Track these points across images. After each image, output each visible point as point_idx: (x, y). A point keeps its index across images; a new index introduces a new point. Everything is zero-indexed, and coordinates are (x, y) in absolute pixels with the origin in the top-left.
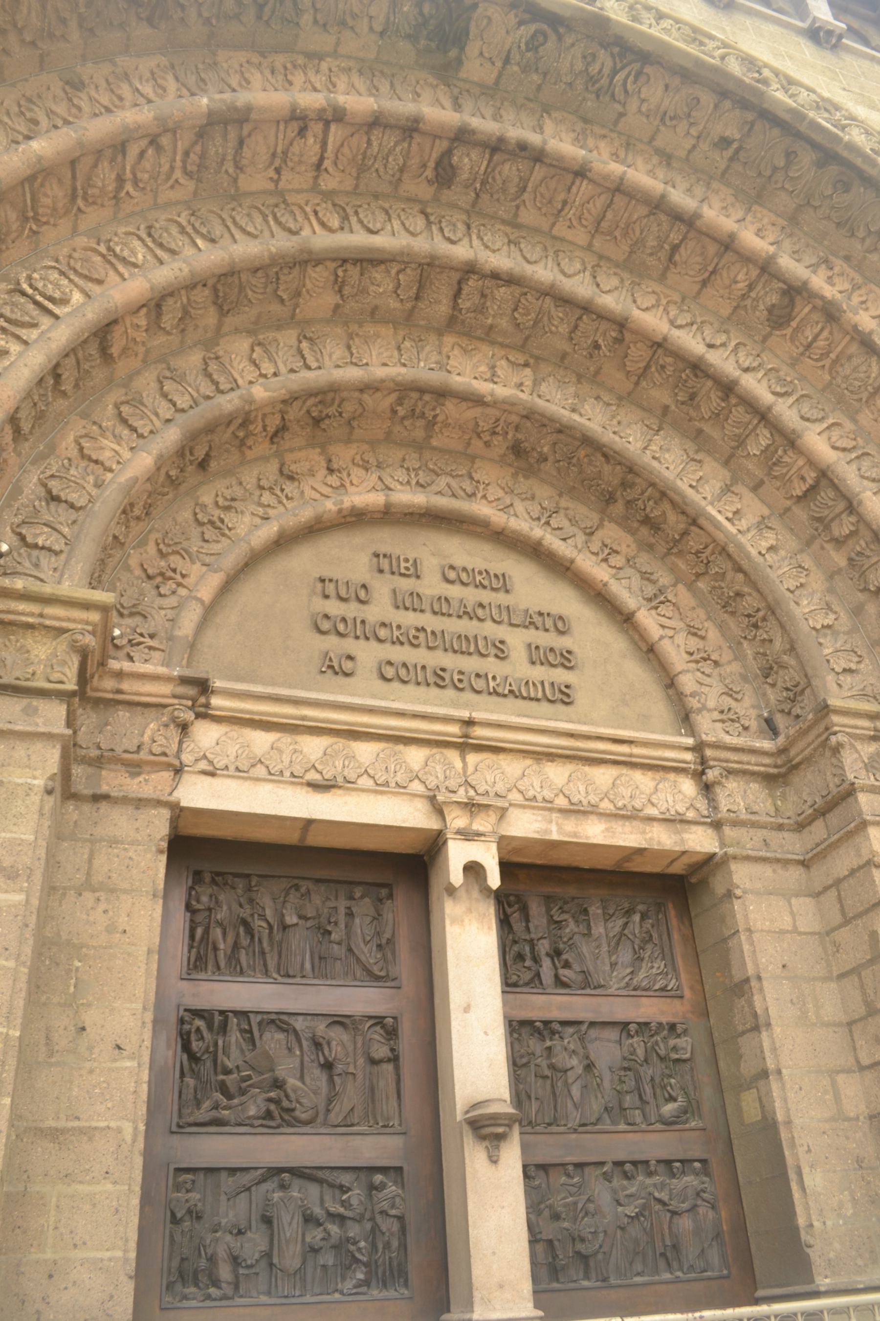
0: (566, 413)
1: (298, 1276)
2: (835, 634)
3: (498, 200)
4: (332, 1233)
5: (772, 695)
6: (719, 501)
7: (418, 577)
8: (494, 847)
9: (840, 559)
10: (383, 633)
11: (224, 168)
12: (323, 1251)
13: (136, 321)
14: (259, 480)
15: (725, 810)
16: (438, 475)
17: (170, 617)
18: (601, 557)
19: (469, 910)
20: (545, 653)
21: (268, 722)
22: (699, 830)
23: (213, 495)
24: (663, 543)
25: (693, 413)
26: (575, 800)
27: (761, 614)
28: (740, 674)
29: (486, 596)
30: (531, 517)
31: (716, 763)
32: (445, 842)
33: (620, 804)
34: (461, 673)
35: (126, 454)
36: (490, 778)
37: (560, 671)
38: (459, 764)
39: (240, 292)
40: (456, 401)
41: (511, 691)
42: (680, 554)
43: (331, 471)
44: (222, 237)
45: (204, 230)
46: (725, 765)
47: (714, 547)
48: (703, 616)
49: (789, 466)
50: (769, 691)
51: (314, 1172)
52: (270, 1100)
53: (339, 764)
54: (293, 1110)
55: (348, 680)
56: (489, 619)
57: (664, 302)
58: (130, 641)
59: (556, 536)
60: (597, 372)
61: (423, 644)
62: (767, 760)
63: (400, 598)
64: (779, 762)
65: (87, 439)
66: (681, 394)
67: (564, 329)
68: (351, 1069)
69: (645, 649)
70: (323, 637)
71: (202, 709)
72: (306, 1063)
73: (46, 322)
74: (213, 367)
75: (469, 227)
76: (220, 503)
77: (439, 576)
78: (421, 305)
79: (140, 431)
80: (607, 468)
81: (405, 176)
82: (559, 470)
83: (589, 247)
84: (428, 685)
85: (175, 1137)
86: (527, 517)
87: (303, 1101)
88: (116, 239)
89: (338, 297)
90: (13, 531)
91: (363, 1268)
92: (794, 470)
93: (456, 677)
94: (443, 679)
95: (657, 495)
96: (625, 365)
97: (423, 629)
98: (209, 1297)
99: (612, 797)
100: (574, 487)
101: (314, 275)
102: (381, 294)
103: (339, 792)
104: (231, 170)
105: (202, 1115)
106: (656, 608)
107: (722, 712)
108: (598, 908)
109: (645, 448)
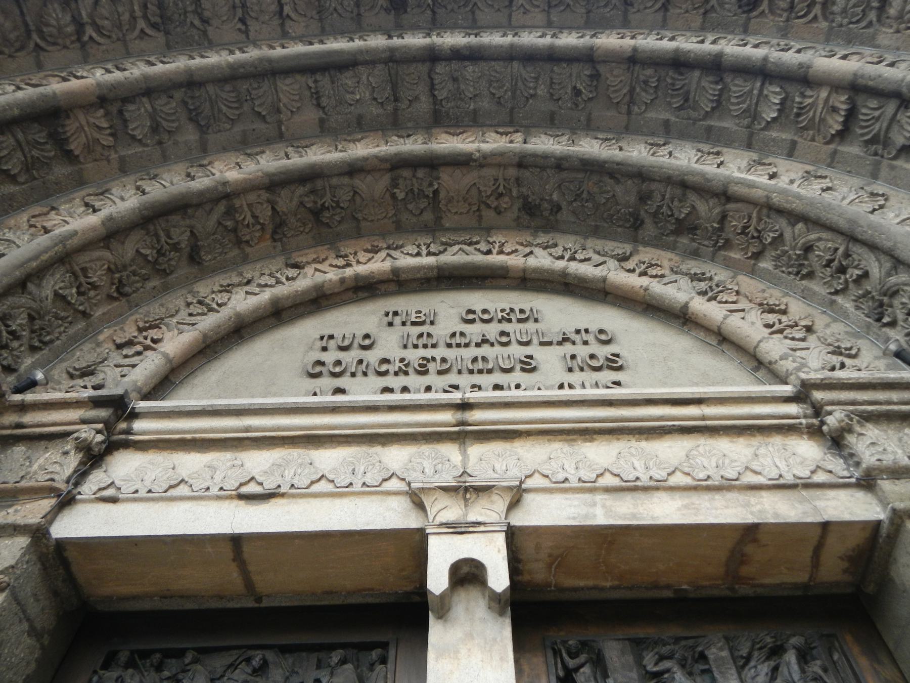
3: (452, 10)
8: (500, 540)
10: (384, 368)
11: (188, 20)
16: (451, 246)
19: (470, 636)
21: (204, 441)
24: (706, 243)
25: (694, 114)
27: (840, 251)
28: (847, 333)
33: (702, 475)
39: (212, 108)
40: (449, 170)
42: (728, 245)
46: (851, 408)
47: (759, 212)
49: (812, 105)
60: (589, 120)
67: (542, 91)
78: (403, 105)
80: (619, 190)
81: (362, 10)
89: (321, 112)
92: (821, 106)
95: (678, 192)
96: (611, 99)
97: (434, 359)
99: (686, 470)
100: (597, 227)
101: (285, 88)
102: (357, 101)
104: (197, 22)
106: (715, 298)
108: (721, 649)
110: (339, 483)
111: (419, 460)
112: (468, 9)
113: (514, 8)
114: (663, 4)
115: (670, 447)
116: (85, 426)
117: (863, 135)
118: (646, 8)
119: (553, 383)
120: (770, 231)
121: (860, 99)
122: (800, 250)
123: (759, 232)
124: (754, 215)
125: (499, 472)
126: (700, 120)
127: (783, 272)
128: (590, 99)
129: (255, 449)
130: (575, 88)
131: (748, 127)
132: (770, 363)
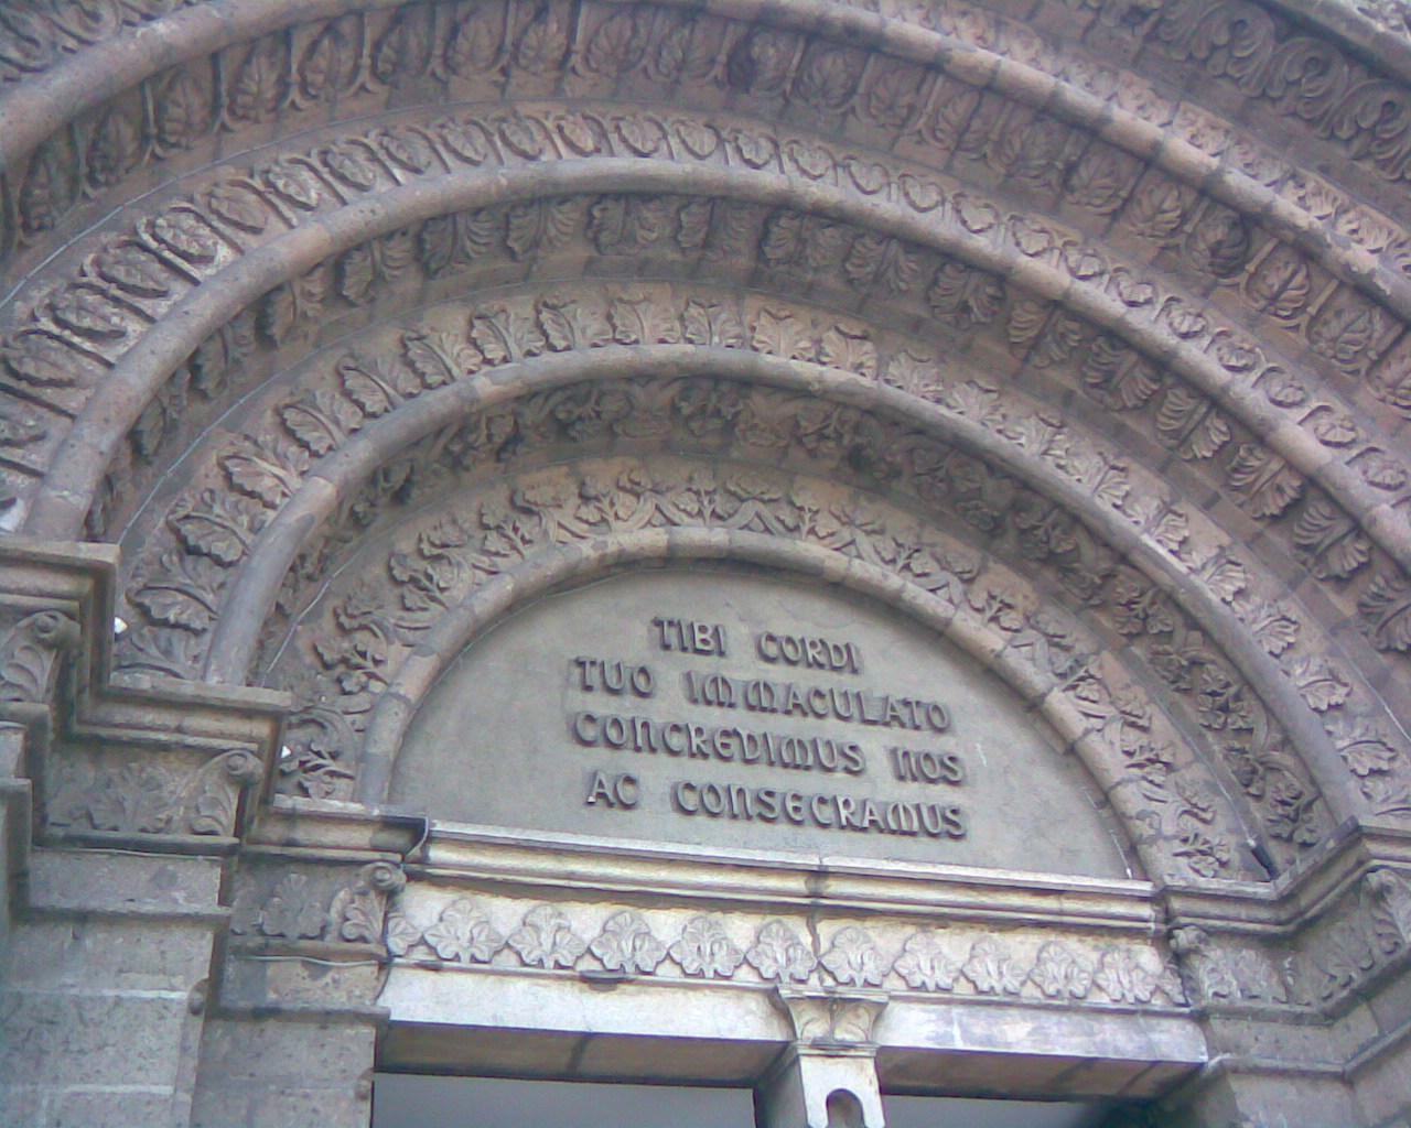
0: (928, 404)
2: (1350, 718)
3: (816, 106)
5: (1258, 812)
6: (1158, 526)
7: (722, 654)
8: (870, 1066)
9: (1345, 605)
10: (676, 741)
11: (430, 68)
13: (308, 287)
14: (481, 515)
15: (1211, 992)
16: (742, 501)
17: (359, 725)
18: (989, 614)
20: (918, 762)
22: (1174, 1026)
23: (414, 540)
24: (1076, 591)
25: (1109, 400)
26: (985, 987)
27: (1232, 690)
28: (1207, 783)
29: (825, 680)
30: (883, 559)
31: (1188, 920)
32: (796, 1061)
33: (1051, 990)
34: (796, 797)
35: (295, 482)
36: (855, 959)
37: (941, 788)
38: (806, 939)
41: (872, 822)
42: (1102, 606)
43: (585, 498)
44: (429, 163)
45: (403, 157)
46: (1201, 922)
47: (1155, 595)
48: (1143, 697)
49: (1254, 470)
50: (1253, 805)
53: (627, 947)
55: (628, 814)
56: (831, 714)
57: (1059, 243)
58: (302, 763)
59: (921, 586)
61: (737, 756)
62: (1264, 914)
63: (697, 687)
64: (1284, 915)
65: (236, 461)
66: (1093, 373)
69: (1060, 749)
70: (586, 750)
71: (415, 867)
73: (179, 289)
74: (415, 351)
75: (776, 146)
76: (426, 552)
77: (753, 651)
79: (314, 447)
80: (990, 484)
82: (918, 488)
83: (947, 170)
84: (749, 818)
86: (876, 558)
88: (277, 169)
90: (129, 601)
92: (1266, 476)
93: (790, 805)
94: (770, 807)
96: (1008, 335)
97: (738, 734)
99: (1038, 979)
101: (559, 216)
103: (630, 988)
106: (1074, 687)
107: (1185, 841)
109: (1045, 453)
111: (768, 940)
112: (839, 111)
113: (906, 131)
114: (1115, 211)
115: (1022, 943)
116: (377, 855)
117: (1298, 536)
118: (1089, 204)
119: (884, 799)
120: (1161, 621)
121: (1312, 493)
122: (1187, 659)
123: (1147, 616)
124: (1150, 594)
126: (1113, 410)
127: (1157, 671)
128: (979, 323)
130: (966, 302)
131: (1170, 449)
132: (1123, 814)
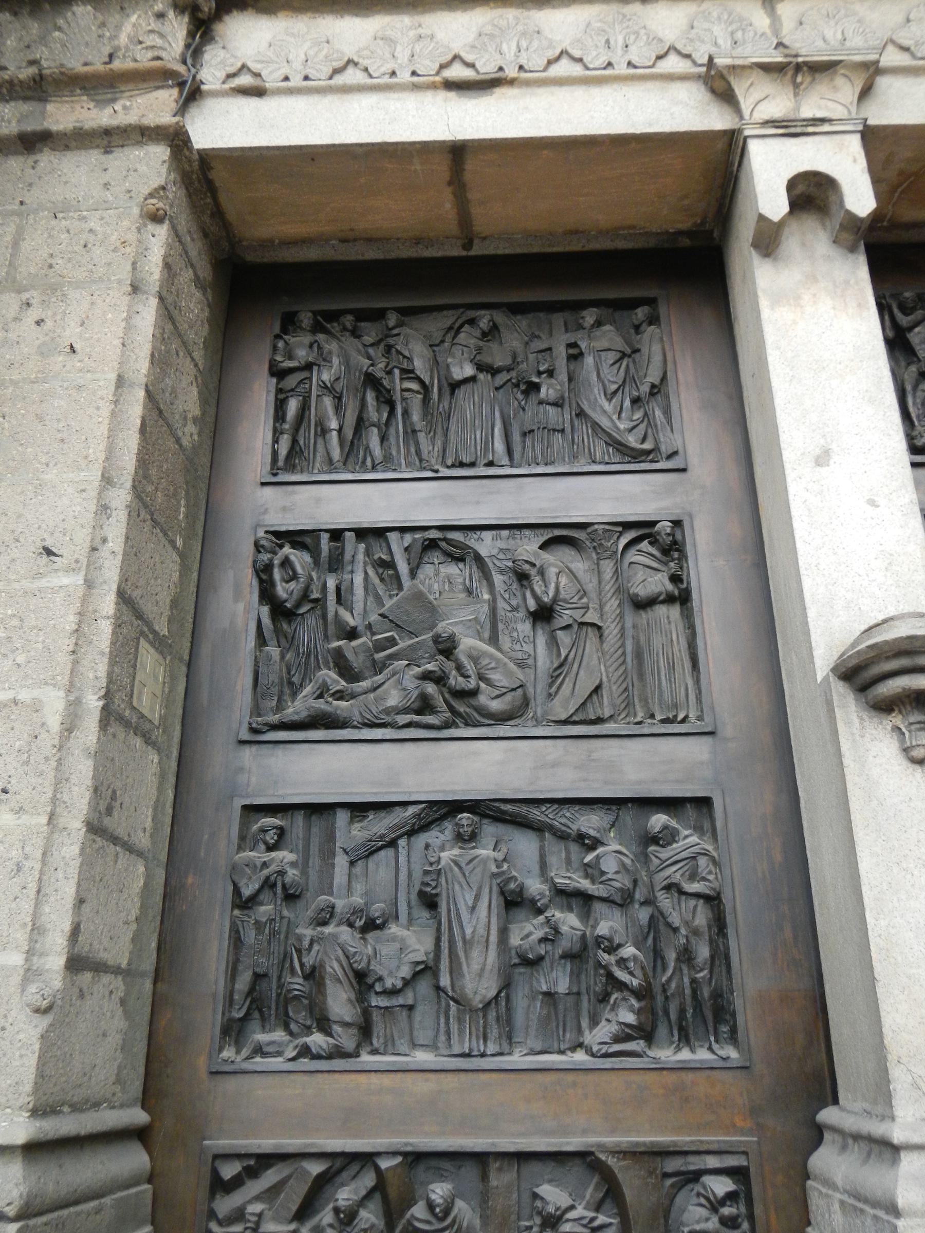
1: (492, 1015)
4: (564, 929)
8: (855, 143)
12: (546, 964)
19: (812, 278)
51: (523, 809)
52: (426, 676)
53: (509, 48)
54: (474, 693)
68: (591, 617)
72: (500, 613)
85: (248, 753)
87: (495, 676)
91: (633, 1001)
98: (305, 1052)
105: (297, 708)
110: (590, 63)
111: (706, 25)
125: (832, 43)
129: (442, 10)
